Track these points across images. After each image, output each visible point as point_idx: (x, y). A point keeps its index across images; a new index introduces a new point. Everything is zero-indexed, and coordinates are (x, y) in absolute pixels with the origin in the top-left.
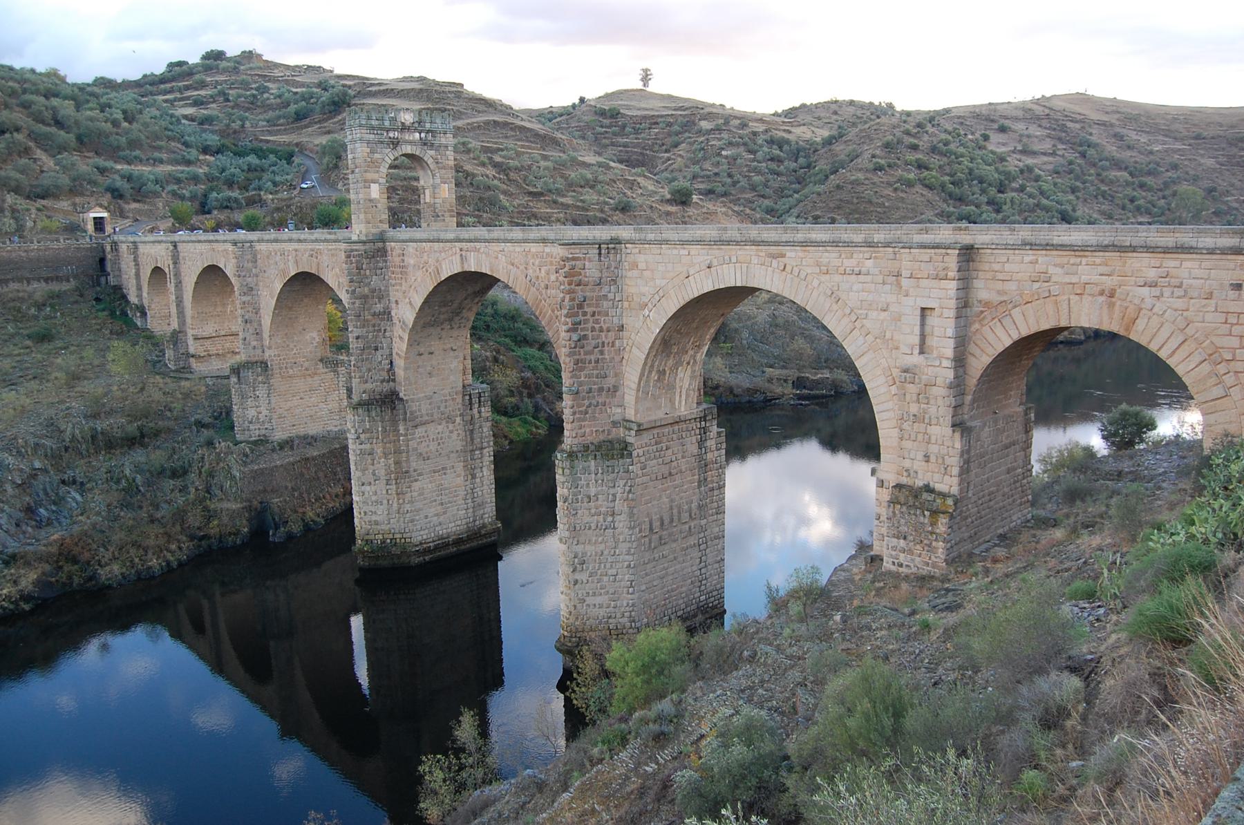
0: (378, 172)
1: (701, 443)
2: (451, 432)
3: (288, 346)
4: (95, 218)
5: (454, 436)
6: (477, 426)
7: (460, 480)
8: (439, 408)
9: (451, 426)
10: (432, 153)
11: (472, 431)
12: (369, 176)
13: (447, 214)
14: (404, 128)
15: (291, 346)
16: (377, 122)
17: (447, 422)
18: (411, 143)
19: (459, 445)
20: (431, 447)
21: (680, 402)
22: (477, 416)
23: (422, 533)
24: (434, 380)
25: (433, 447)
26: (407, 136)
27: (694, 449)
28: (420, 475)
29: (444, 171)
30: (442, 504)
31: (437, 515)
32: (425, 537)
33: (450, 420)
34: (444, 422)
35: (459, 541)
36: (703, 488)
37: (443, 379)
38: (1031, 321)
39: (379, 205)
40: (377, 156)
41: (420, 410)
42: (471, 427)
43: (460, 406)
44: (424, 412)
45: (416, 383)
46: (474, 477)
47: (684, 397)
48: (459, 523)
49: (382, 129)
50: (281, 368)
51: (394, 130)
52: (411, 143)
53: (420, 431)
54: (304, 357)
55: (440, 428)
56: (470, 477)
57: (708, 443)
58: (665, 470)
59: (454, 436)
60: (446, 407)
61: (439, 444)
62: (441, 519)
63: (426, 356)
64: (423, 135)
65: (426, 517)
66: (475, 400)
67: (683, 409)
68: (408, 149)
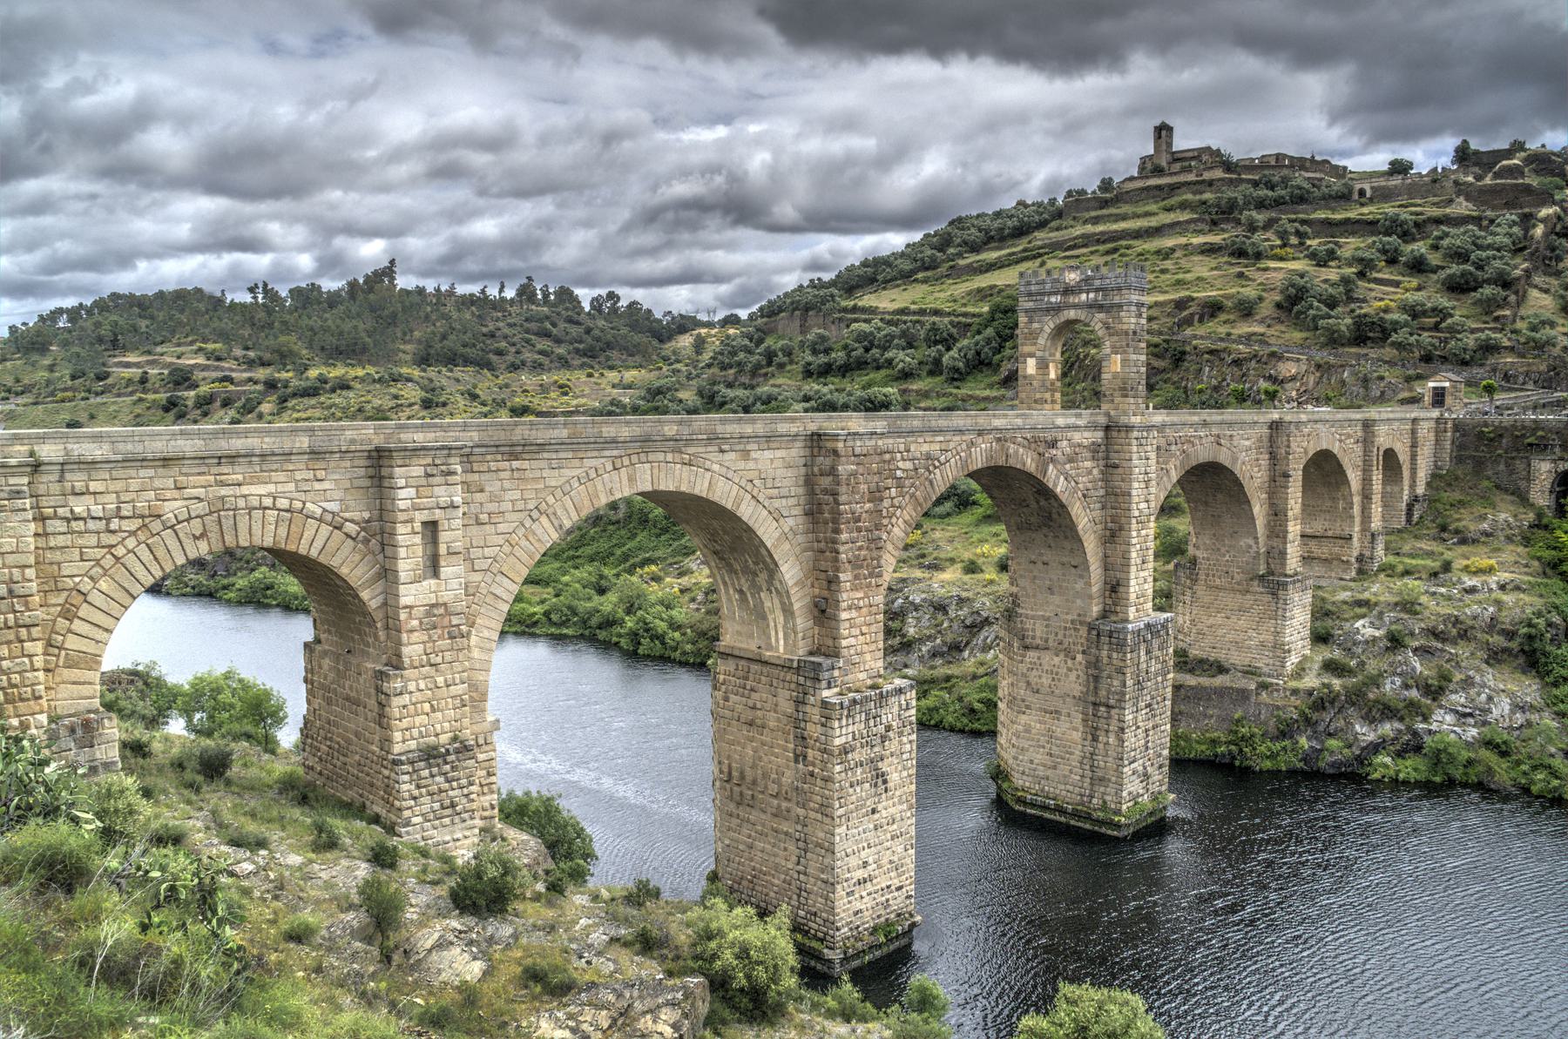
0: (1035, 344)
1: (799, 702)
2: (1070, 670)
3: (1219, 549)
4: (1435, 388)
5: (1073, 676)
6: (1105, 674)
7: (1077, 736)
8: (1056, 634)
9: (1069, 662)
10: (1102, 316)
11: (1096, 679)
12: (1027, 349)
13: (1117, 394)
14: (1068, 291)
15: (1223, 550)
16: (1037, 287)
17: (1066, 656)
18: (1075, 306)
19: (1077, 689)
20: (1044, 680)
21: (777, 640)
22: (1105, 660)
23: (1025, 778)
24: (1056, 599)
25: (1046, 680)
26: (1072, 299)
27: (788, 707)
28: (1028, 707)
29: (1116, 338)
30: (1051, 755)
31: (1044, 766)
32: (1027, 784)
33: (1069, 654)
34: (1062, 656)
35: (1060, 810)
36: (801, 766)
37: (1067, 600)
38: (318, 544)
39: (1035, 383)
40: (1036, 325)
41: (1033, 630)
42: (1095, 672)
43: (1083, 640)
44: (1038, 634)
45: (1034, 596)
46: (1095, 739)
47: (781, 635)
48: (1071, 788)
49: (1043, 294)
50: (1207, 575)
51: (1055, 293)
52: (1075, 306)
53: (1032, 655)
54: (1239, 567)
55: (1056, 660)
56: (1090, 737)
57: (808, 709)
58: (749, 715)
59: (1073, 676)
60: (1065, 636)
61: (1053, 679)
62: (1049, 773)
63: (1040, 565)
64: (1092, 295)
65: (1031, 762)
66: (1104, 639)
67: (781, 649)
68: (1072, 314)
